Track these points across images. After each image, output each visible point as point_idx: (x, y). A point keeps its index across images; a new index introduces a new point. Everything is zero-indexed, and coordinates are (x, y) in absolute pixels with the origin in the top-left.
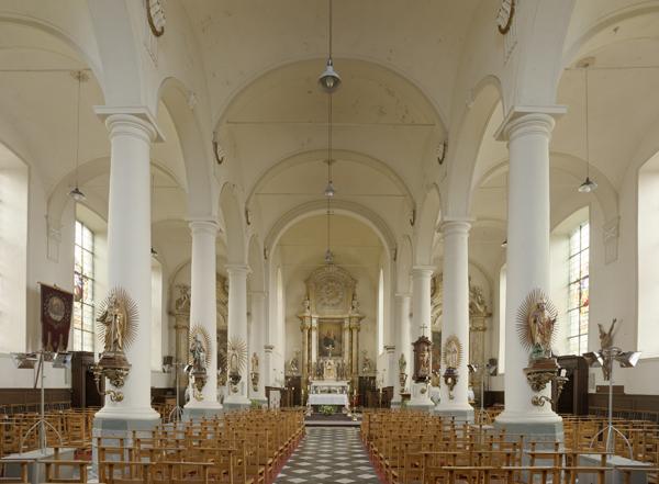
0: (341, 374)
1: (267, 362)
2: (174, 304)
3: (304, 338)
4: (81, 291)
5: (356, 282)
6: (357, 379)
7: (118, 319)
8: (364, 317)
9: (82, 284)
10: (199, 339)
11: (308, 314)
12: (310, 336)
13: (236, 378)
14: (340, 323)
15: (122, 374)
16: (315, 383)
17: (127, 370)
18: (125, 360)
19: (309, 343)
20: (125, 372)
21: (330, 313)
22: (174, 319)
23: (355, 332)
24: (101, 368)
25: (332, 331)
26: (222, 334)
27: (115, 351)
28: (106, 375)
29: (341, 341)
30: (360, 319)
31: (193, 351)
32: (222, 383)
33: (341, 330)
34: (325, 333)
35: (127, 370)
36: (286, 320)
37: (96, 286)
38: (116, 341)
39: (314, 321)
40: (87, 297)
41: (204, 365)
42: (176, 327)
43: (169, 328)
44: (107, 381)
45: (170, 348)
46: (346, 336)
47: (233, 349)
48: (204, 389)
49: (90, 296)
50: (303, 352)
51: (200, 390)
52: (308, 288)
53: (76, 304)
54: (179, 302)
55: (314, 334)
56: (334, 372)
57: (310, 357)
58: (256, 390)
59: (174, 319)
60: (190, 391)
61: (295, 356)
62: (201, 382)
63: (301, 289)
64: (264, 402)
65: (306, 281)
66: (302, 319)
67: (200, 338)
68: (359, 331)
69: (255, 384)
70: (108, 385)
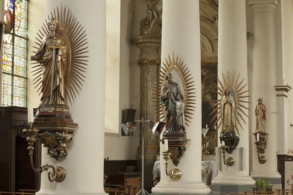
1: (280, 114)
2: (138, 26)
4: (13, 17)
7: (61, 58)
9: (14, 8)
10: (174, 80)
13: (231, 142)
15: (64, 140)
17: (71, 133)
18: (69, 117)
20: (69, 136)
22: (138, 51)
24: (36, 130)
26: (209, 69)
27: (55, 105)
28: (44, 141)
31: (165, 100)
32: (208, 151)
35: (71, 133)
37: (32, 10)
38: (57, 89)
40: (20, 24)
41: (182, 121)
42: (141, 63)
43: (131, 64)
44: (44, 150)
45: (132, 97)
47: (227, 94)
48: (182, 160)
49: (23, 24)
51: (176, 163)
53: (7, 38)
54: (145, 23)
58: (262, 161)
59: (138, 51)
60: (161, 164)
62: (177, 150)
64: (274, 181)
67: (176, 78)
69: (261, 150)
70: (45, 158)
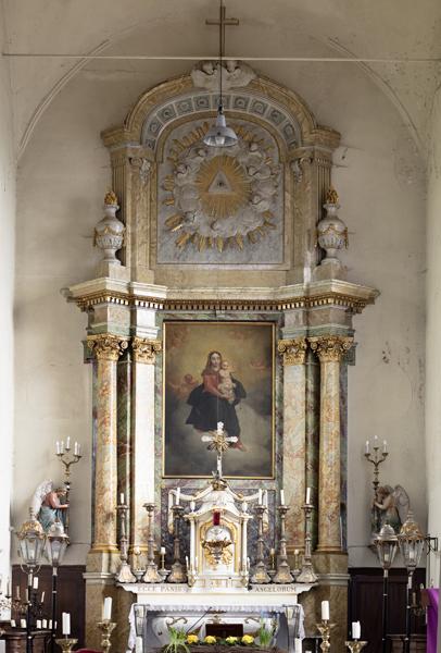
0: (266, 560)
3: (98, 392)
5: (335, 139)
6: (337, 578)
8: (371, 300)
11: (116, 279)
12: (125, 383)
14: (263, 325)
16: (153, 596)
19: (125, 416)
21: (222, 279)
23: (330, 368)
25: (230, 359)
29: (268, 406)
30: (355, 305)
33: (271, 357)
34: (194, 368)
36: (19, 313)
39: (147, 319)
46: (294, 380)
50: (96, 450)
52: (118, 166)
55: (146, 374)
56: (238, 551)
57: (125, 481)
61: (55, 472)
63: (84, 173)
65: (110, 137)
66: (90, 305)
68: (347, 358)
